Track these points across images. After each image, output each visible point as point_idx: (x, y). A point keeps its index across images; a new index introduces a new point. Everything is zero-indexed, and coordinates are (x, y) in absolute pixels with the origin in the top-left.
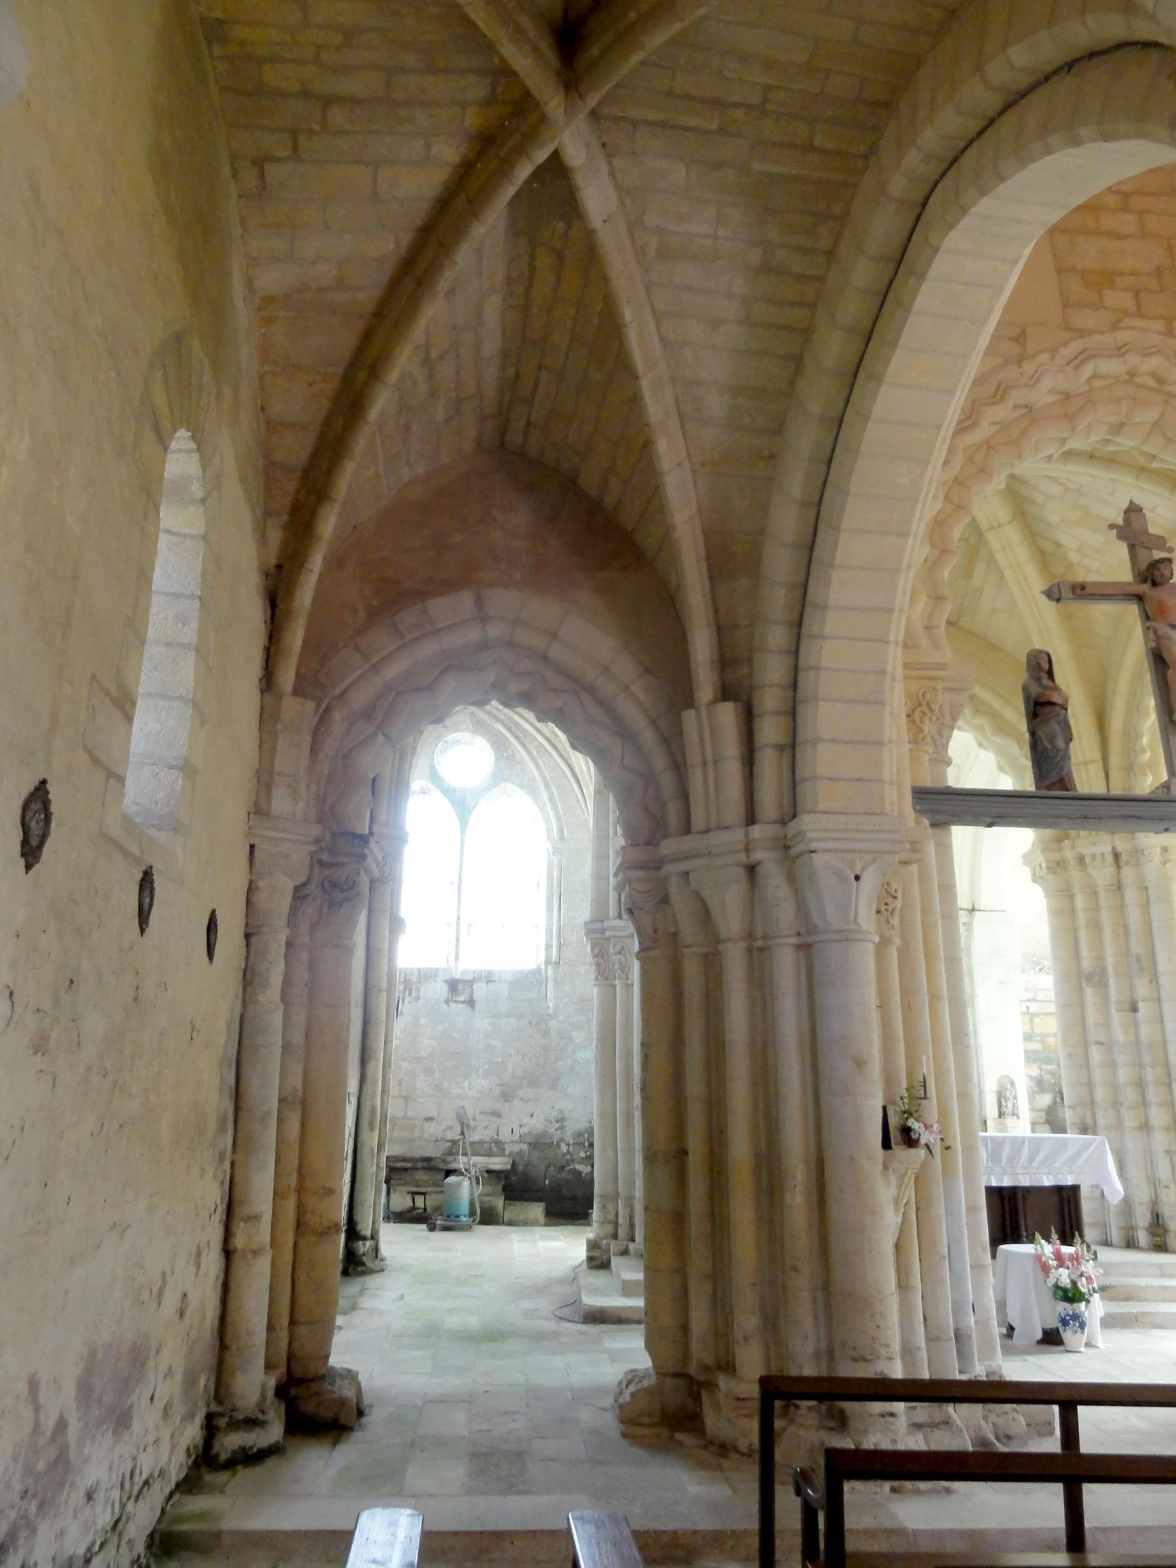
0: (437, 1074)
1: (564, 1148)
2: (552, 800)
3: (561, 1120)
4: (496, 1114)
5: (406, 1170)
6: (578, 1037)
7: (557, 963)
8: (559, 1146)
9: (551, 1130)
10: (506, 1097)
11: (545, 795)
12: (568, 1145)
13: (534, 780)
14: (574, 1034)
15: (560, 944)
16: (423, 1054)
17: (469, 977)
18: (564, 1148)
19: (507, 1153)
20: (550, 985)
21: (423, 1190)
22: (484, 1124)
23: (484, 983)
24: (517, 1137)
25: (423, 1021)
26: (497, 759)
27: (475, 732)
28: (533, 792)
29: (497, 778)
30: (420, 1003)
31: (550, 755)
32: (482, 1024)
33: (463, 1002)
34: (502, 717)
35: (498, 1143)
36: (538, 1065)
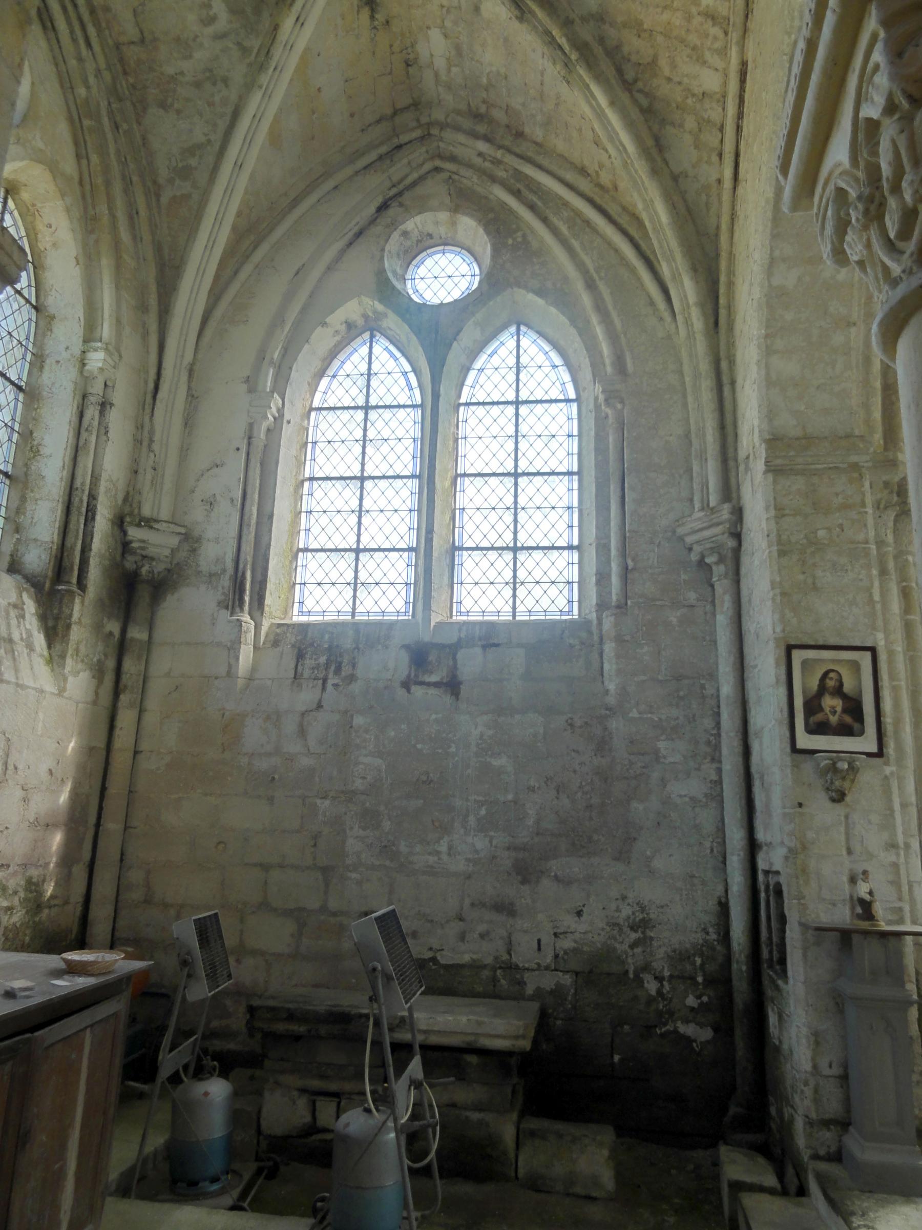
0: (387, 825)
1: (652, 987)
2: (600, 308)
3: (642, 925)
4: (505, 908)
5: (298, 1038)
6: (672, 751)
7: (622, 607)
8: (639, 981)
9: (622, 948)
10: (526, 871)
11: (586, 299)
12: (659, 979)
13: (566, 279)
14: (661, 745)
15: (625, 572)
16: (359, 784)
17: (450, 638)
18: (652, 987)
19: (530, 990)
20: (609, 648)
21: (333, 1087)
22: (482, 928)
23: (478, 650)
24: (549, 959)
25: (359, 720)
26: (496, 252)
27: (456, 209)
28: (562, 299)
29: (493, 283)
30: (356, 687)
31: (595, 231)
32: (473, 727)
33: (436, 685)
34: (501, 174)
35: (510, 968)
36: (589, 807)
